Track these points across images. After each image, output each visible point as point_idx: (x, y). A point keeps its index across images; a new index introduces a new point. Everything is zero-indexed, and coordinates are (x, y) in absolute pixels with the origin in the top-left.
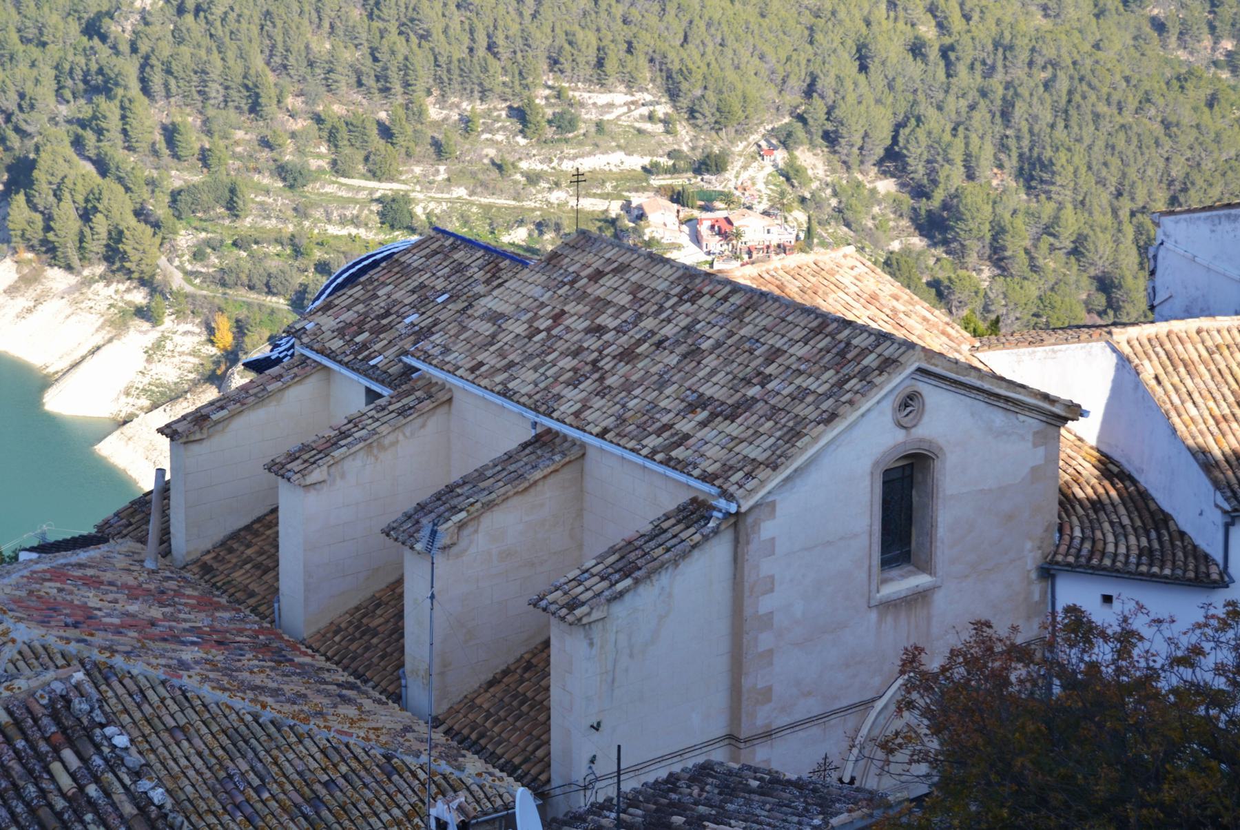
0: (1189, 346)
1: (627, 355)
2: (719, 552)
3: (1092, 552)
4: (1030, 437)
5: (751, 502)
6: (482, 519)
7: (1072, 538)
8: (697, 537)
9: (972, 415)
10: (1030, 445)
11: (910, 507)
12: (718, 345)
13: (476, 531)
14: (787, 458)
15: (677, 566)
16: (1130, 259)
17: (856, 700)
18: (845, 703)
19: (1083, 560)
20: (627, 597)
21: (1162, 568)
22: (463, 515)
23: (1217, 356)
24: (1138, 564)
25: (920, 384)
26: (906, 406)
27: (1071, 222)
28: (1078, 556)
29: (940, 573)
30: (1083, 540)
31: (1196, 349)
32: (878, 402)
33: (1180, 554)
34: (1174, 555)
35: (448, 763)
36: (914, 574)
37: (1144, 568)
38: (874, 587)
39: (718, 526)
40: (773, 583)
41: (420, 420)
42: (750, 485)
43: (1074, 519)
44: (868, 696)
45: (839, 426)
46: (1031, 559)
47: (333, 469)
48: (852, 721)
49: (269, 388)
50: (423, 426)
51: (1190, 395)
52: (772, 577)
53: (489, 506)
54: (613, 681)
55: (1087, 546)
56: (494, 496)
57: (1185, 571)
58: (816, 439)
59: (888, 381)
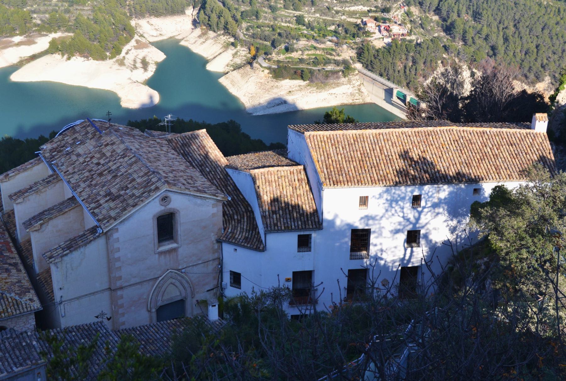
0: (273, 176)
1: (101, 175)
2: (101, 242)
3: (231, 237)
5: (107, 229)
6: (49, 222)
7: (228, 232)
8: (92, 238)
9: (189, 201)
10: (211, 207)
11: (172, 225)
12: (122, 175)
13: (48, 225)
14: (120, 217)
15: (86, 246)
16: (501, 41)
17: (153, 278)
18: (148, 279)
19: (227, 240)
20: (69, 255)
21: (248, 244)
22: (42, 221)
23: (280, 180)
24: (242, 242)
25: (169, 194)
26: (165, 199)
27: (485, 30)
28: (227, 238)
29: (180, 243)
30: (230, 232)
31: (275, 177)
32: (153, 199)
33: (255, 240)
34: (254, 239)
35: (19, 297)
36: (172, 243)
37: (243, 244)
38: (156, 248)
39: (99, 235)
41: (53, 185)
42: (108, 224)
43: (231, 226)
44: (157, 276)
45: (137, 208)
46: (214, 238)
47: (25, 199)
48: (151, 283)
49: (28, 167)
50: (55, 186)
51: (267, 192)
52: (119, 248)
53: (51, 219)
54: (67, 276)
55: (230, 235)
56: (52, 216)
57: (254, 246)
58: (129, 212)
59: (155, 194)
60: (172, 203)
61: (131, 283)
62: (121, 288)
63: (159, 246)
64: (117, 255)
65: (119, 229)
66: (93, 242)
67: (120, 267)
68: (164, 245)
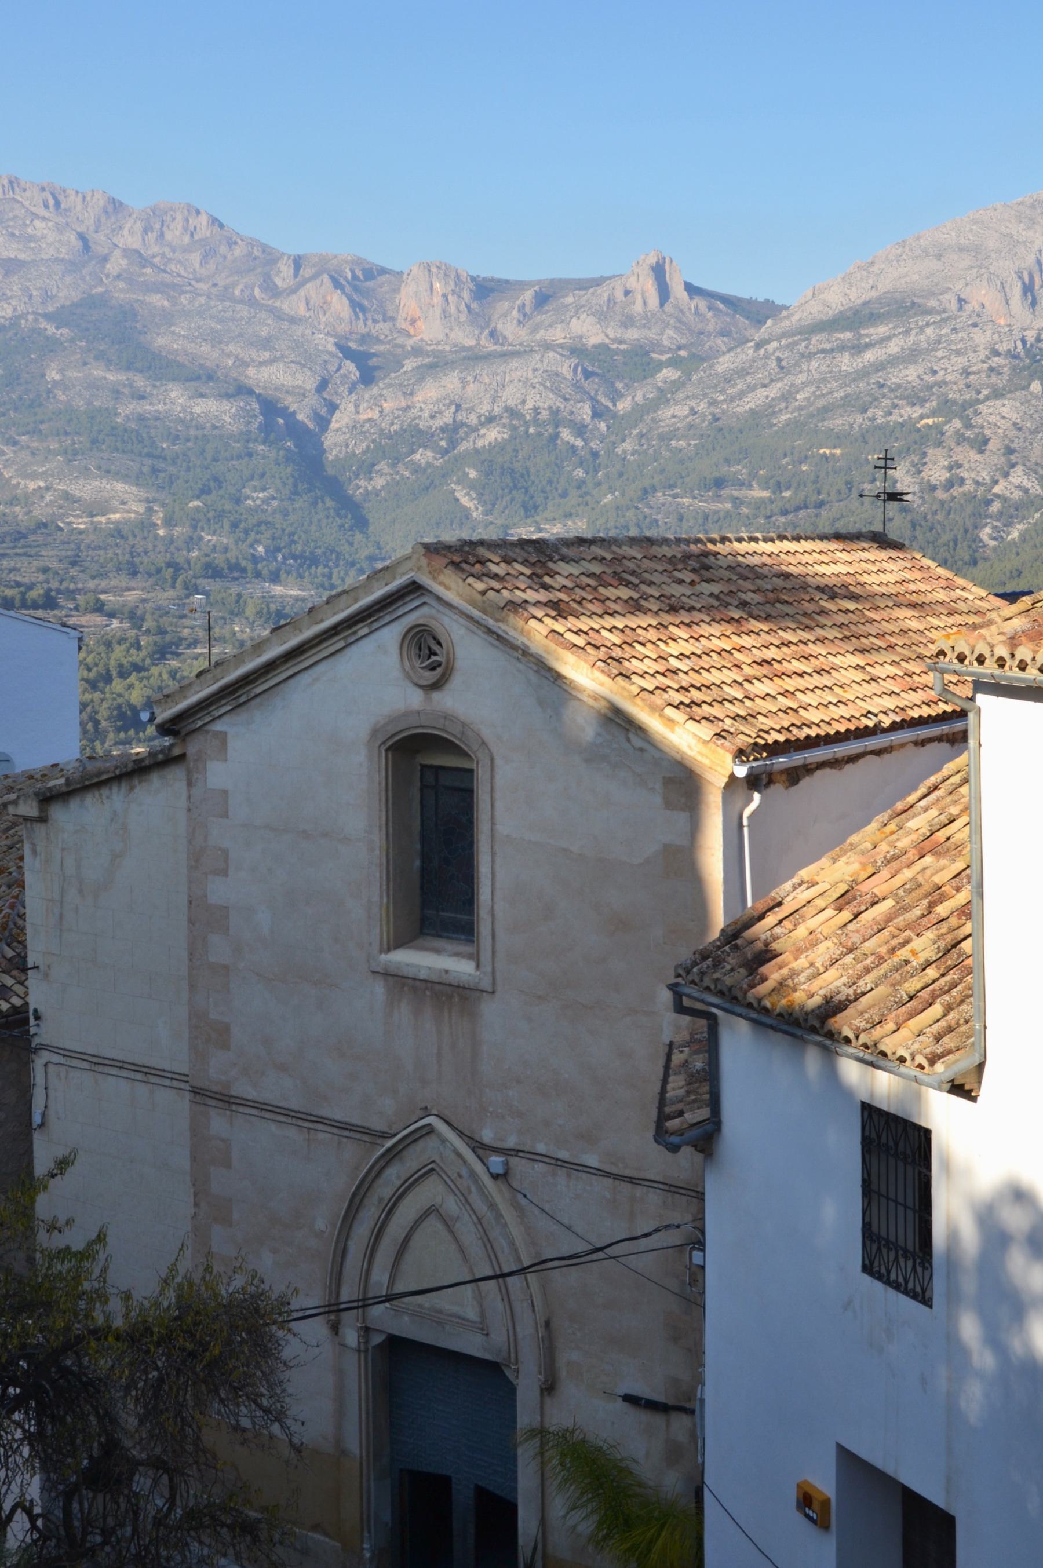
4: (658, 786)
10: (658, 800)
40: (226, 860)
52: (225, 852)
60: (456, 681)
61: (267, 1096)
62: (227, 1101)
63: (399, 942)
64: (219, 891)
65: (233, 744)
66: (155, 779)
67: (226, 967)
68: (438, 951)
